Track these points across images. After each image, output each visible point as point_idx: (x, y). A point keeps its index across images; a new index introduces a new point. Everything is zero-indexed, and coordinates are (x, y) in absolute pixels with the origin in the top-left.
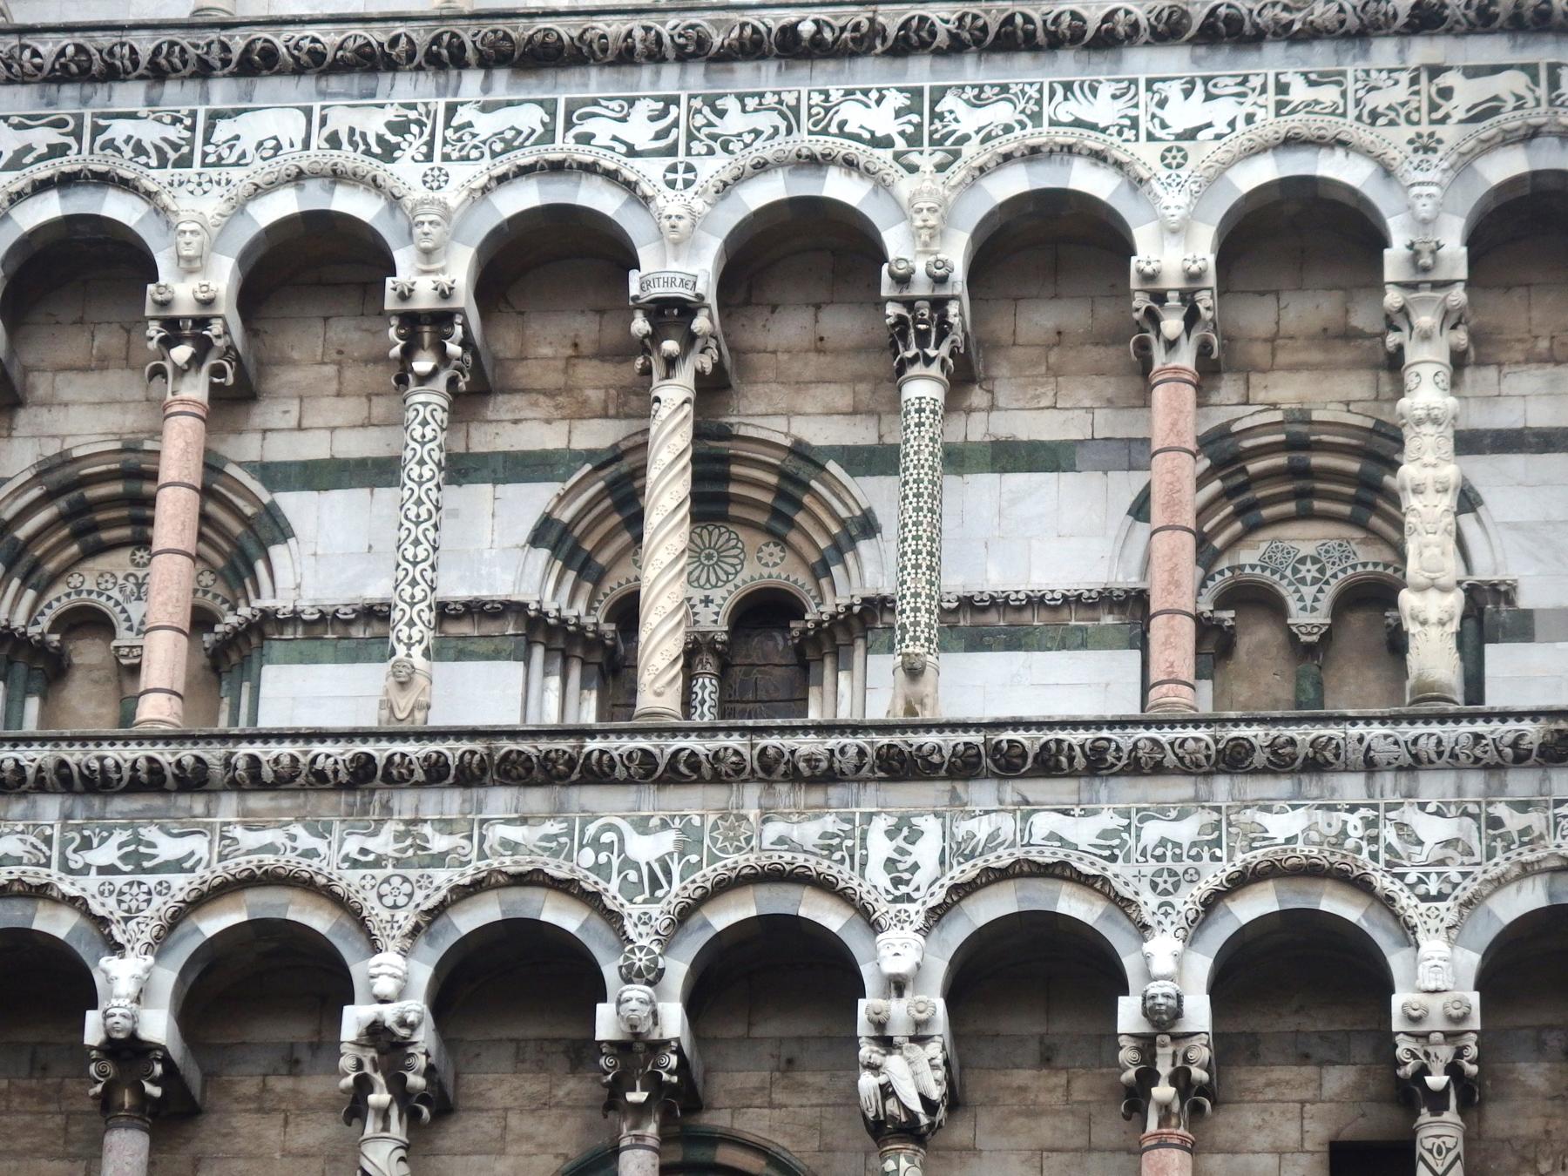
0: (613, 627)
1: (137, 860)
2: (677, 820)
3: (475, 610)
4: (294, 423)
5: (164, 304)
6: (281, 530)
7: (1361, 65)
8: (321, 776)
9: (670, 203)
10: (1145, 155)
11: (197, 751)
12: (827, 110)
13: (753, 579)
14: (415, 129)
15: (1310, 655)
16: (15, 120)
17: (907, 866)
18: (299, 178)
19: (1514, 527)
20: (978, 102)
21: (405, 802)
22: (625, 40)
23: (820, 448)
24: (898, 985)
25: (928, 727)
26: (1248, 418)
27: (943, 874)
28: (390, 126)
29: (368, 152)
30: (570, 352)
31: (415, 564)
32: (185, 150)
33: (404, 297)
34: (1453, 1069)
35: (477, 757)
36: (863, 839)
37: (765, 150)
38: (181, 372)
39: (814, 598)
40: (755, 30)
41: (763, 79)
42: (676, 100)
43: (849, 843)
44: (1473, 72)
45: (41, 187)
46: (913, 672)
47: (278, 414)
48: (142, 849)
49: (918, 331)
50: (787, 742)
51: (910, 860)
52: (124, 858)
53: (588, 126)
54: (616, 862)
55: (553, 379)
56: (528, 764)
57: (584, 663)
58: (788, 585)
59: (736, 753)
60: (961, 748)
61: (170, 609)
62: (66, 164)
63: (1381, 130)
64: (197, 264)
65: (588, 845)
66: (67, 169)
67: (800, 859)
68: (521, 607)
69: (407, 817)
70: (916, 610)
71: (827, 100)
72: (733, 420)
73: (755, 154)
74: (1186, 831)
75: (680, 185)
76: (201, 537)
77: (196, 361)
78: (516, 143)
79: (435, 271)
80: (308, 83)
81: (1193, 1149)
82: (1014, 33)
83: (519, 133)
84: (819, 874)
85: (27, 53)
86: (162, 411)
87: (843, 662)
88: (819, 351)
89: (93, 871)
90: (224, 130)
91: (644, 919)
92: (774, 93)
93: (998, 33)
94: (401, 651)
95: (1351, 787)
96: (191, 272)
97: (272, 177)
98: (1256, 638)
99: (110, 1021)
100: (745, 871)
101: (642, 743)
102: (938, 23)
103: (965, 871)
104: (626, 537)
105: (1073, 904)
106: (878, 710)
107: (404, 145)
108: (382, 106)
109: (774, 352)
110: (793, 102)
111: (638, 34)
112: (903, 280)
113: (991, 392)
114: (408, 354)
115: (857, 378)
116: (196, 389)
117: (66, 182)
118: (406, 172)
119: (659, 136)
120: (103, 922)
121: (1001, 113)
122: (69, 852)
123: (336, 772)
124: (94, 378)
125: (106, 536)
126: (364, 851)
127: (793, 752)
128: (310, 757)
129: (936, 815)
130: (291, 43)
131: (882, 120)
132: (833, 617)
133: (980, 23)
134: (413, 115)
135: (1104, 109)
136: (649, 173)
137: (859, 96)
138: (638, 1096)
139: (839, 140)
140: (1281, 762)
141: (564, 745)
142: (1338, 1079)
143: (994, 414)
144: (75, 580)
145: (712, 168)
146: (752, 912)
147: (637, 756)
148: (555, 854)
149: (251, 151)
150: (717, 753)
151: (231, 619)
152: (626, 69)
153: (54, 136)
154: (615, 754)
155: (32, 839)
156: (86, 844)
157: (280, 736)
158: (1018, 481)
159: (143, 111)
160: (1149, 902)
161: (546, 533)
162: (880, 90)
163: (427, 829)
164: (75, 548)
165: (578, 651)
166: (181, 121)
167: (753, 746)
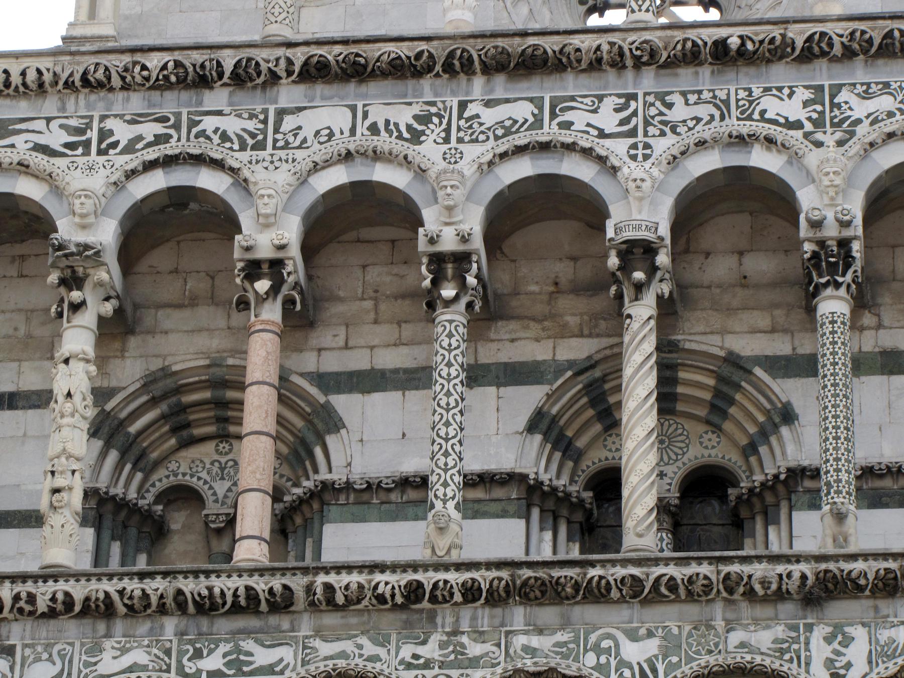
0: (591, 494)
2: (660, 630)
4: (342, 343)
5: (248, 249)
6: (335, 424)
8: (381, 599)
9: (630, 170)
11: (286, 580)
12: (751, 102)
13: (696, 458)
14: (435, 120)
16: (128, 118)
17: (843, 664)
18: (348, 157)
20: (866, 95)
21: (446, 617)
22: (595, 52)
23: (748, 358)
25: (853, 557)
27: (871, 670)
28: (416, 118)
29: (400, 137)
30: (552, 289)
31: (447, 440)
32: (260, 137)
33: (432, 241)
35: (503, 582)
36: (807, 643)
37: (703, 132)
38: (261, 300)
39: (744, 472)
40: (694, 44)
41: (701, 81)
42: (634, 97)
43: (795, 646)
46: (840, 517)
47: (329, 338)
48: (242, 657)
49: (828, 263)
50: (746, 569)
51: (844, 660)
52: (228, 665)
53: (568, 116)
54: (613, 663)
55: (539, 309)
56: (543, 588)
57: (569, 522)
58: (724, 463)
59: (706, 577)
60: (882, 572)
61: (258, 476)
64: (272, 220)
65: (591, 650)
66: (170, 152)
67: (758, 659)
68: (523, 477)
69: (447, 629)
70: (838, 470)
71: (750, 95)
72: (679, 337)
73: (696, 135)
75: (640, 158)
77: (275, 290)
78: (514, 129)
79: (454, 221)
80: (352, 87)
82: (893, 44)
83: (516, 122)
84: (773, 671)
85: (138, 69)
86: (247, 331)
87: (770, 518)
88: (743, 286)
90: (289, 123)
92: (709, 91)
93: (881, 44)
94: (439, 505)
96: (267, 226)
100: (715, 669)
102: (834, 37)
107: (428, 132)
108: (410, 104)
109: (709, 287)
110: (724, 97)
111: (605, 47)
112: (816, 225)
113: (879, 316)
114: (436, 283)
115: (775, 306)
116: (272, 313)
117: (169, 162)
118: (430, 151)
119: (622, 123)
121: (885, 103)
122: (185, 660)
123: (393, 596)
124: (186, 313)
126: (415, 656)
127: (750, 577)
128: (373, 584)
129: (864, 625)
130: (341, 58)
131: (794, 109)
132: (763, 484)
133: (867, 36)
134: (434, 110)
136: (617, 149)
137: (774, 92)
139: (761, 124)
143: (881, 331)
144: (173, 466)
145: (663, 145)
147: (628, 581)
148: (566, 657)
149: (310, 138)
150: (691, 577)
151: (298, 491)
152: (595, 74)
154: (611, 579)
155: (155, 651)
156: (198, 654)
157: (349, 568)
159: (227, 110)
161: (539, 423)
162: (790, 87)
163: (465, 639)
165: (565, 512)
166: (257, 117)
167: (718, 573)
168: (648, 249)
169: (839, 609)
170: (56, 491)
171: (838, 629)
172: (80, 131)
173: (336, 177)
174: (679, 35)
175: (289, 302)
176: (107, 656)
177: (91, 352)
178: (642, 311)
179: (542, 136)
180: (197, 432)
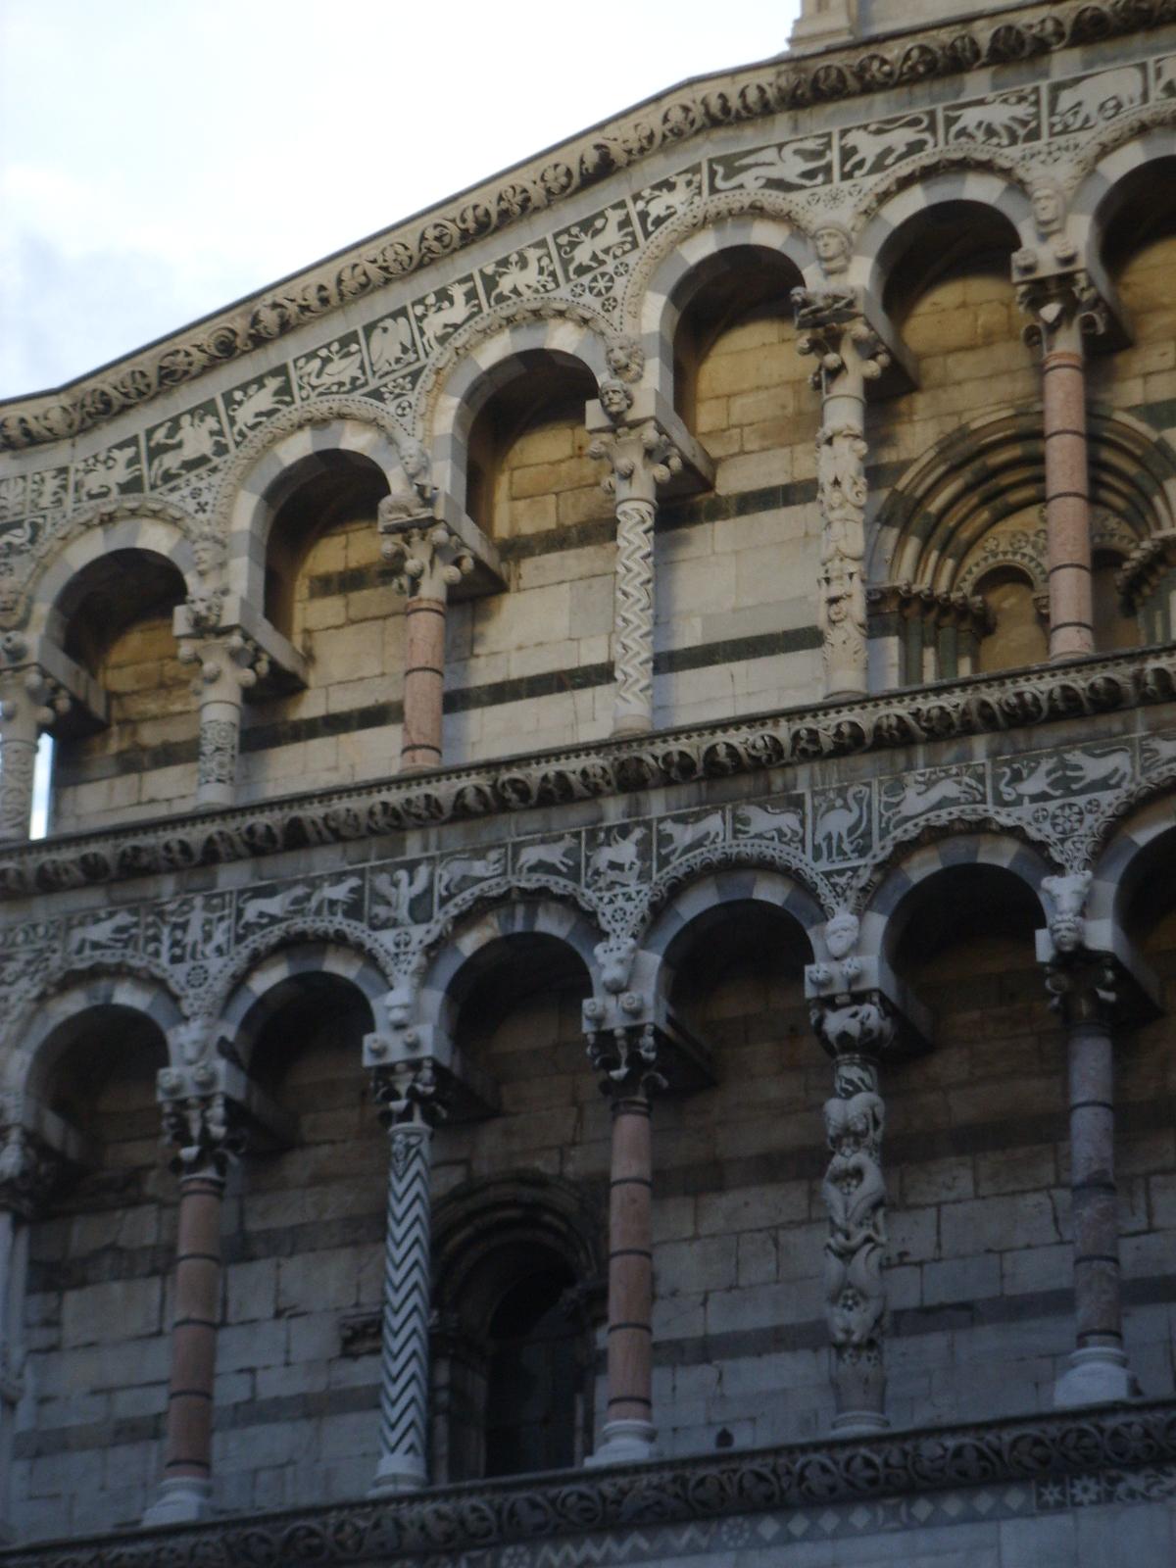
1: (1065, 783)
16: (873, 127)
32: (1033, 124)
38: (1053, 328)
45: (905, 183)
48: (1070, 773)
52: (1053, 784)
61: (1069, 548)
64: (1055, 226)
80: (1138, 40)
85: (876, 65)
86: (1040, 370)
89: (1026, 800)
90: (1067, 99)
97: (1115, 135)
99: (1057, 936)
116: (1068, 343)
117: (926, 175)
120: (1041, 847)
122: (1002, 787)
144: (991, 544)
149: (1094, 114)
151: (1136, 555)
155: (966, 779)
156: (1017, 777)
159: (990, 96)
164: (985, 515)
170: (833, 601)
175: (1088, 324)
176: (910, 793)
177: (857, 426)
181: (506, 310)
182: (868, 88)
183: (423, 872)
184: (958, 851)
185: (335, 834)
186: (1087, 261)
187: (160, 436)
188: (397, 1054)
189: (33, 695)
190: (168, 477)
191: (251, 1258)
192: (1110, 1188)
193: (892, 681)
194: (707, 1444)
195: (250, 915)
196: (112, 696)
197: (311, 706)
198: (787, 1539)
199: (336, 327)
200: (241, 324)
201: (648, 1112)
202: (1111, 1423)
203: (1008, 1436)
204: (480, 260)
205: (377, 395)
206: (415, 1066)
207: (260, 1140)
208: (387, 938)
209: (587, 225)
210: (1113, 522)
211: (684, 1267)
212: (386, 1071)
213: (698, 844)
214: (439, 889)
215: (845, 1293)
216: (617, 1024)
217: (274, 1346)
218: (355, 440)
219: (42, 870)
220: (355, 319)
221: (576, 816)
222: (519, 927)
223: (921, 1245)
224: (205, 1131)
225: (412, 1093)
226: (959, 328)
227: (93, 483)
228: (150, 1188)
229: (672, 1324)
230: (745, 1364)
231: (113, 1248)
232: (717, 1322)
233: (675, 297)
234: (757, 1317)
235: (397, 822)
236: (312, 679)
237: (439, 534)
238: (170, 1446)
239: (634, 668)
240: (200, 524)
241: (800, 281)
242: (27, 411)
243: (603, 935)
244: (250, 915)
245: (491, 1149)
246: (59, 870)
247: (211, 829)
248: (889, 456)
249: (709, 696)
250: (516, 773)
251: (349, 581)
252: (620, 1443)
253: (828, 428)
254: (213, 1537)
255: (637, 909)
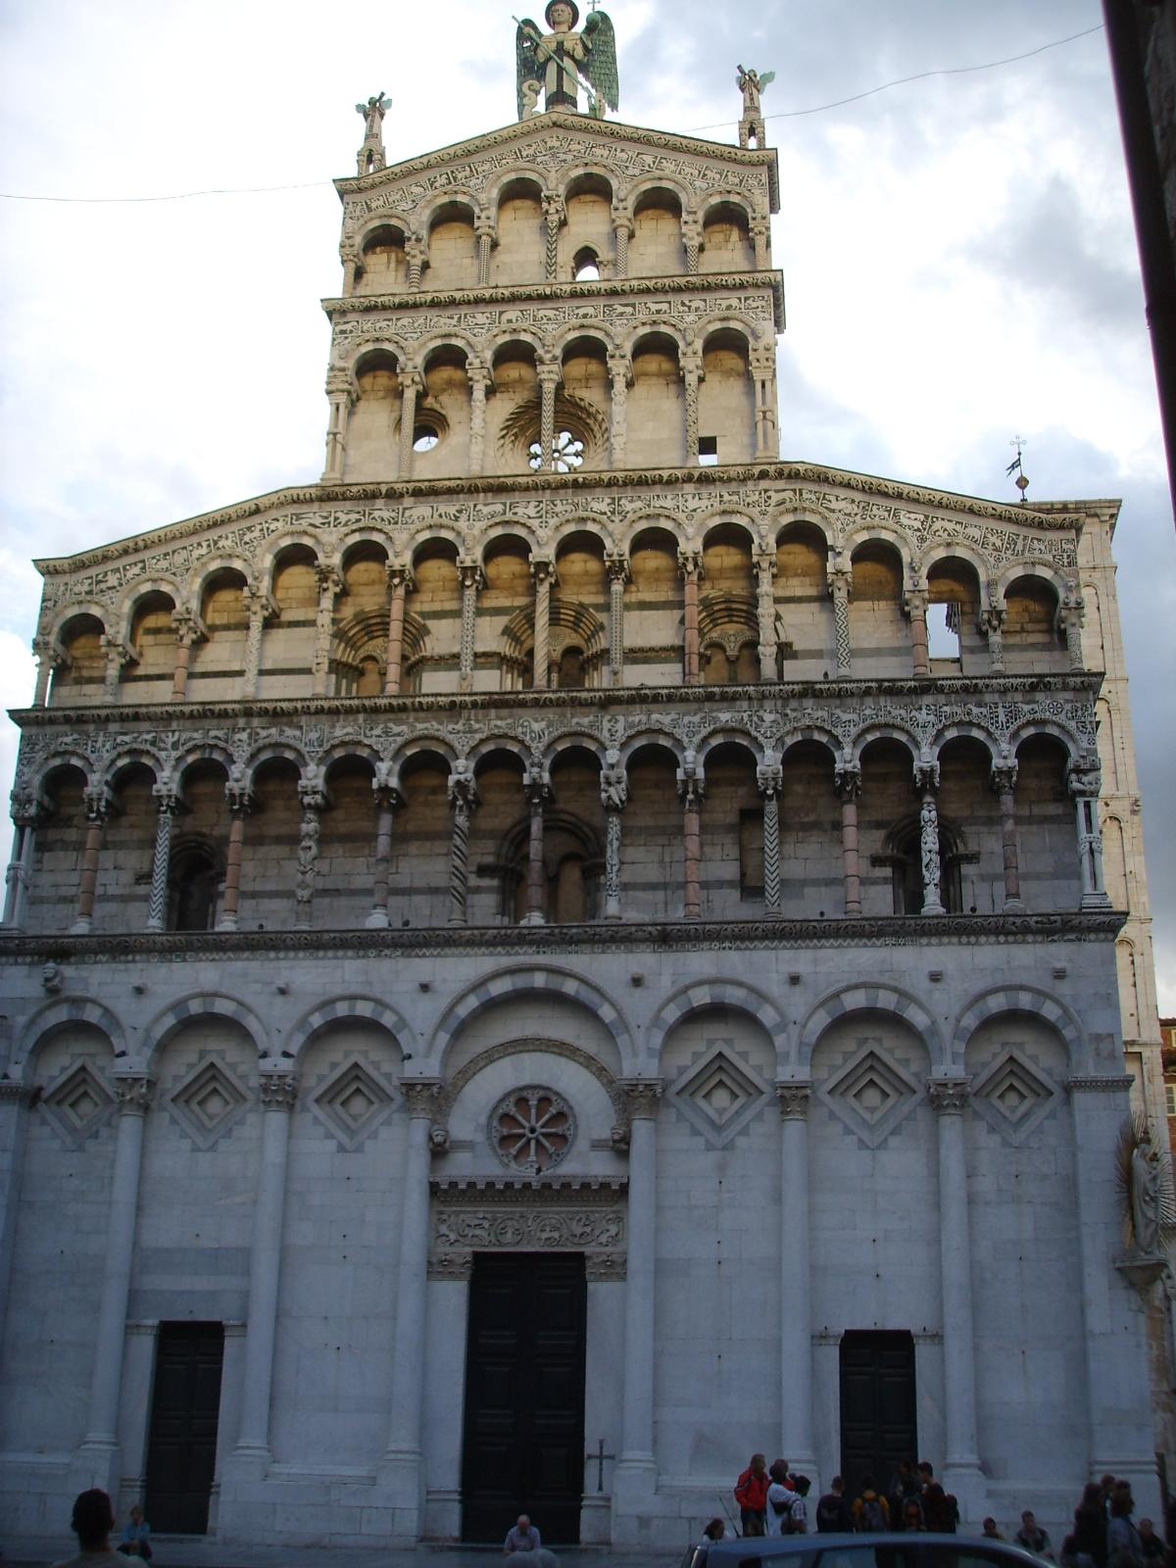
1: (386, 733)
3: (485, 654)
6: (428, 632)
7: (745, 489)
9: (540, 533)
10: (681, 516)
15: (732, 662)
19: (792, 626)
20: (631, 501)
21: (465, 713)
24: (612, 766)
25: (619, 690)
26: (713, 594)
34: (774, 788)
37: (569, 516)
38: (396, 586)
44: (777, 491)
45: (353, 531)
50: (578, 695)
53: (516, 510)
62: (361, 525)
63: (751, 508)
74: (696, 719)
76: (404, 634)
77: (401, 582)
80: (432, 498)
81: (699, 813)
86: (390, 599)
91: (537, 748)
95: (745, 704)
98: (718, 658)
101: (536, 696)
103: (632, 732)
104: (529, 631)
105: (663, 741)
106: (605, 685)
112: (610, 556)
114: (464, 580)
116: (400, 592)
117: (361, 530)
118: (462, 524)
120: (377, 752)
121: (638, 504)
125: (376, 634)
131: (603, 507)
135: (669, 503)
136: (535, 523)
138: (536, 801)
140: (724, 697)
141: (513, 696)
142: (742, 791)
145: (553, 522)
146: (569, 745)
151: (413, 659)
153: (357, 516)
156: (372, 729)
157: (428, 695)
158: (646, 613)
160: (685, 740)
164: (366, 638)
168: (547, 564)
169: (614, 709)
171: (613, 716)
172: (326, 518)
173: (426, 535)
174: (559, 477)
175: (407, 586)
176: (337, 729)
177: (331, 608)
178: (543, 589)
179: (506, 518)
180: (376, 634)
181: (219, 552)
182: (345, 499)
183: (177, 734)
184: (350, 749)
185: (149, 718)
186: (409, 567)
187: (100, 577)
188: (164, 792)
189: (50, 657)
190: (102, 591)
191: (108, 849)
192: (387, 861)
193: (332, 694)
194: (256, 929)
195: (118, 741)
196: (74, 658)
197: (140, 671)
198: (278, 959)
199: (163, 549)
200: (131, 545)
201: (244, 820)
202: (382, 934)
203: (351, 935)
204: (213, 535)
205: (174, 574)
206: (170, 796)
207: (115, 812)
208: (163, 754)
209: (249, 529)
210: (406, 646)
211: (248, 868)
212: (160, 797)
213: (267, 737)
214: (182, 741)
215: (303, 885)
216: (237, 792)
217: (115, 877)
218: (165, 588)
219: (50, 717)
220: (169, 548)
221: (228, 723)
222: (207, 756)
223: (325, 869)
224: (98, 809)
225: (168, 805)
226: (364, 578)
227: (76, 589)
228: (75, 822)
229: (247, 886)
230: (266, 901)
231: (63, 841)
232: (258, 886)
233: (275, 556)
234: (271, 886)
235: (170, 717)
236: (141, 662)
237: (191, 624)
238: (78, 907)
239: (252, 674)
240: (112, 608)
241: (317, 558)
242: (57, 563)
243: (235, 762)
244: (118, 741)
245: (189, 823)
246: (56, 718)
247: (108, 711)
248: (338, 616)
249: (277, 690)
250: (211, 707)
251: (157, 631)
252: (226, 924)
253: (321, 608)
254: (94, 939)
255: (247, 755)
